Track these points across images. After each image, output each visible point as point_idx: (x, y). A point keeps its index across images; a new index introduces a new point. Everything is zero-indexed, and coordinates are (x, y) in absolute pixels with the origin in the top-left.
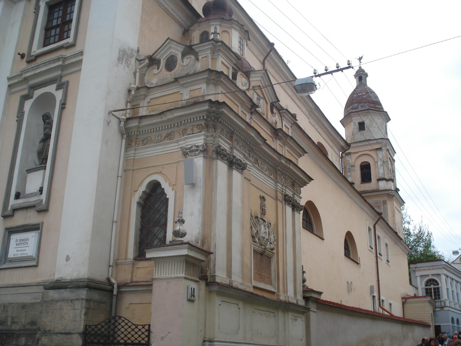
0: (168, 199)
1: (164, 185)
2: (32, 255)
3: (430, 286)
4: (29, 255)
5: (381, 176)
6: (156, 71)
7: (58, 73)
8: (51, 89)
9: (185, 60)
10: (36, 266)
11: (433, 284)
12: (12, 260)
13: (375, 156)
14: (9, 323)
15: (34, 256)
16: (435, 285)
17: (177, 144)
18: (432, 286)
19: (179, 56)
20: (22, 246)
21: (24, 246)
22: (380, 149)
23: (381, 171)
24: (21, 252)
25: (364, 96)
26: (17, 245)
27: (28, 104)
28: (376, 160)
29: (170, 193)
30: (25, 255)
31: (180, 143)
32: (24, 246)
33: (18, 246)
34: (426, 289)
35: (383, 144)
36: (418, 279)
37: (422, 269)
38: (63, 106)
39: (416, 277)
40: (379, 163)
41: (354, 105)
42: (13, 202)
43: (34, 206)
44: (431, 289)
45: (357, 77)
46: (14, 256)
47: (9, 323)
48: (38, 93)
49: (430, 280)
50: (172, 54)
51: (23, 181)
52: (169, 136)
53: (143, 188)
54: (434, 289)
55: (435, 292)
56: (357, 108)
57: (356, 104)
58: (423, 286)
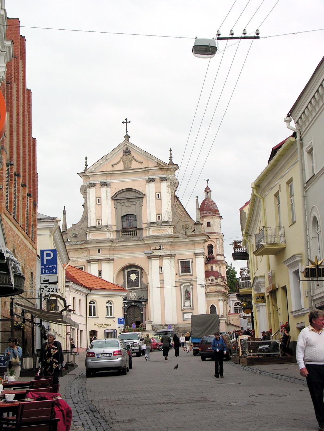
3: (237, 306)
5: (218, 253)
7: (190, 281)
8: (189, 284)
11: (239, 305)
12: (185, 319)
13: (215, 242)
14: (189, 330)
16: (239, 305)
18: (238, 306)
19: (214, 279)
22: (218, 238)
23: (218, 250)
25: (210, 207)
27: (182, 287)
28: (216, 244)
29: (216, 307)
34: (235, 308)
35: (220, 236)
36: (231, 302)
37: (233, 297)
38: (193, 289)
39: (230, 301)
40: (217, 245)
41: (205, 212)
42: (183, 307)
44: (237, 308)
45: (206, 193)
47: (189, 330)
48: (184, 285)
49: (237, 303)
51: (184, 303)
52: (215, 296)
54: (239, 307)
55: (239, 309)
56: (207, 214)
57: (206, 211)
58: (234, 306)
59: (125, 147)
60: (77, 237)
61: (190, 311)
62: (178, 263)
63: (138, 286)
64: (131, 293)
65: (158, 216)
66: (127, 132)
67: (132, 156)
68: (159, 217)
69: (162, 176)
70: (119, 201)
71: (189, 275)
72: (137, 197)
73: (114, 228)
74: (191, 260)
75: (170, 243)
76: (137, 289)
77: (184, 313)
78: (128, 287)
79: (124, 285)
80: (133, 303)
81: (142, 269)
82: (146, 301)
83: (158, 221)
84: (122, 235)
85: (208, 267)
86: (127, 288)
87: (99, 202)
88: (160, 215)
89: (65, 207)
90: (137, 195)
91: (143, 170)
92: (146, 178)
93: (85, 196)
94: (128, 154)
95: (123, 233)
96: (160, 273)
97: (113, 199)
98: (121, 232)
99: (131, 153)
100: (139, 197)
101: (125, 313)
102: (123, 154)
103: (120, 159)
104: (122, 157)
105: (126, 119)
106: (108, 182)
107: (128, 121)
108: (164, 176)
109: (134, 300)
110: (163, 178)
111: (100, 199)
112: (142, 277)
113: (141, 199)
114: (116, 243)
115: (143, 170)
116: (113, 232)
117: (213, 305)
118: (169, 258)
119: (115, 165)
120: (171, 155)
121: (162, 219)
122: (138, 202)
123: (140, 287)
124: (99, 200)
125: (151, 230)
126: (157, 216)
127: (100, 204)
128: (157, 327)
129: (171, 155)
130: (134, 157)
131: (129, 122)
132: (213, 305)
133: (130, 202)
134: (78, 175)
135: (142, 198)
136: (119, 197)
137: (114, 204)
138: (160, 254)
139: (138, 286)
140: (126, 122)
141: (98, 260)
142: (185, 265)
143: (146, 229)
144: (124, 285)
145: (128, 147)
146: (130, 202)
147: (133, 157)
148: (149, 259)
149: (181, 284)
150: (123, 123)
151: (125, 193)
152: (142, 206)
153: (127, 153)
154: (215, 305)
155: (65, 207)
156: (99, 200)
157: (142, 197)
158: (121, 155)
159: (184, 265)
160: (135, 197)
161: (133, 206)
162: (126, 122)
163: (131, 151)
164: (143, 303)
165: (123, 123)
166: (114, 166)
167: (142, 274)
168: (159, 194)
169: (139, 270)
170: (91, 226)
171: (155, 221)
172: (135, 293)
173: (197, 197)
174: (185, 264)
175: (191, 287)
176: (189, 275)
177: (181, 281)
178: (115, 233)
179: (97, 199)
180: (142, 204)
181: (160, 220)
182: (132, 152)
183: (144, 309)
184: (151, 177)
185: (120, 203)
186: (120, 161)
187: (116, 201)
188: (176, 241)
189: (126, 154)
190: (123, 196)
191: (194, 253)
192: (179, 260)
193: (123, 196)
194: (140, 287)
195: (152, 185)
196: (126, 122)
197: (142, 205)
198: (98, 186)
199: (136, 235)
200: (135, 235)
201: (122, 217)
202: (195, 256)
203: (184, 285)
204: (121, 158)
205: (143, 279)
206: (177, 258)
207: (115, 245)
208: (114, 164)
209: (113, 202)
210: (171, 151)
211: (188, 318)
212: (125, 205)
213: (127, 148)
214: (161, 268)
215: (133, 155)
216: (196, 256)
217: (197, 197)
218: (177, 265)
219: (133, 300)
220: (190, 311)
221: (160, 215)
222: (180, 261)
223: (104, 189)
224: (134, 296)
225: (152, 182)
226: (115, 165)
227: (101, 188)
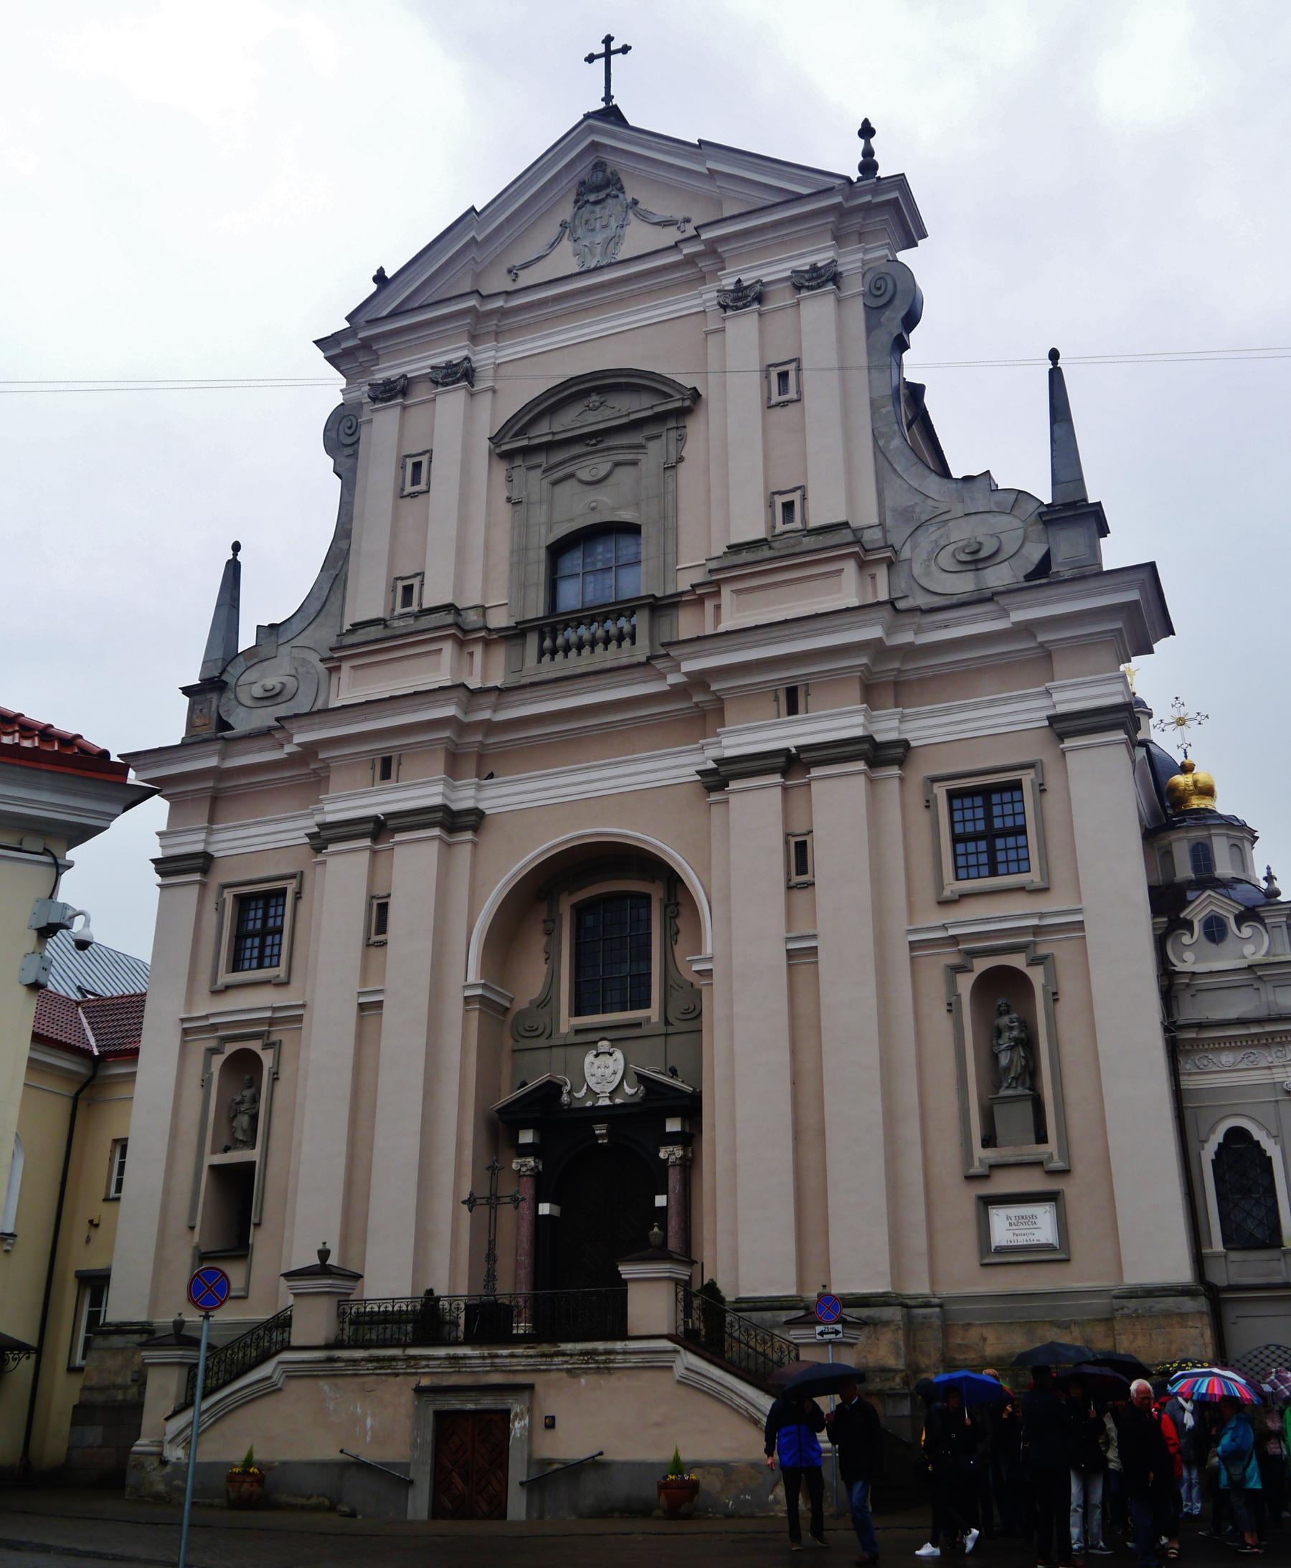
0: (1270, 1158)
1: (1258, 1134)
2: (1051, 1242)
4: (1043, 1241)
6: (1186, 939)
9: (1243, 928)
10: (1067, 1261)
12: (1001, 1250)
15: (1056, 1244)
17: (1267, 1072)
20: (1022, 1227)
21: (1027, 1227)
24: (1025, 1237)
26: (1010, 1224)
27: (965, 984)
29: (1271, 1148)
30: (1035, 1242)
31: (1274, 1071)
32: (1027, 1227)
33: (1014, 1227)
38: (1055, 997)
43: (1039, 1164)
46: (1009, 1244)
50: (1213, 913)
53: (1218, 1137)
59: (588, 162)
60: (279, 700)
61: (1033, 1182)
62: (929, 804)
63: (646, 1004)
64: (589, 1058)
65: (780, 500)
66: (608, 97)
67: (629, 200)
68: (788, 507)
69: (803, 264)
70: (541, 459)
71: (1021, 889)
72: (649, 413)
73: (499, 620)
74: (1027, 778)
75: (864, 660)
76: (639, 1025)
77: (988, 1201)
78: (578, 1011)
79: (547, 1001)
80: (600, 1130)
81: (672, 881)
82: (691, 1107)
83: (777, 531)
84: (542, 653)
85: (1167, 854)
86: (567, 1023)
87: (416, 480)
88: (796, 497)
89: (236, 547)
90: (639, 406)
91: (685, 251)
92: (705, 297)
93: (350, 462)
94: (602, 195)
95: (547, 643)
96: (789, 888)
97: (505, 448)
98: (532, 641)
99: (621, 189)
100: (657, 410)
101: (545, 1209)
102: (576, 202)
103: (559, 229)
104: (568, 219)
105: (608, 40)
106: (484, 357)
107: (614, 46)
108: (822, 259)
109: (607, 1102)
110: (814, 268)
111: (424, 459)
112: (671, 936)
113: (672, 424)
114: (492, 698)
115: (688, 250)
116: (487, 643)
117: (1237, 1136)
118: (860, 765)
119: (525, 266)
120: (868, 153)
121: (804, 520)
122: (653, 447)
123: (653, 1013)
124: (417, 466)
125: (726, 591)
126: (771, 505)
127: (422, 487)
128: (756, 1316)
129: (868, 153)
130: (641, 206)
131: (625, 49)
132: (1237, 1136)
133: (608, 449)
134: (320, 354)
135: (683, 413)
136: (542, 432)
137: (510, 480)
138: (791, 744)
139: (646, 1004)
140: (609, 51)
141: (370, 826)
142: (989, 818)
143: (700, 601)
144: (547, 1001)
145: (608, 157)
146: (608, 449)
147: (635, 202)
148: (715, 797)
149: (955, 960)
150: (591, 58)
151: (578, 408)
152: (682, 466)
153: (598, 189)
154: (1262, 1126)
155: (236, 547)
156: (417, 466)
157: (678, 404)
158: (566, 211)
159: (980, 813)
160: (633, 417)
161: (624, 474)
162: (608, 54)
163: (622, 176)
164: (673, 1126)
165: (591, 58)
166: (519, 272)
167: (677, 915)
168: (791, 368)
169: (657, 893)
170: (359, 618)
171: (757, 531)
172: (618, 1055)
173: (1054, 355)
174: (988, 807)
175: (1037, 976)
176: (1021, 889)
177: (955, 940)
178: (500, 655)
179: (410, 462)
180: (680, 450)
181: (797, 524)
182: (626, 183)
183: (674, 1178)
184: (728, 283)
185: (544, 465)
186: (558, 240)
187: (518, 462)
188: (906, 637)
189: (592, 198)
190: (570, 421)
191: (1052, 719)
192: (936, 785)
193: (570, 421)
194: (653, 1013)
195: (744, 327)
196: (609, 51)
197: (681, 459)
198: (421, 393)
199: (633, 643)
200: (626, 643)
201: (558, 550)
202: (1061, 737)
203: (982, 965)
204: (564, 225)
205: (679, 949)
206: (922, 769)
207: (486, 715)
208: (518, 263)
209: (501, 469)
210: (867, 131)
211: (1021, 1241)
212: (572, 476)
213: (599, 166)
214: (801, 848)
215: (631, 192)
216: (1068, 743)
217: (1054, 355)
218: (920, 818)
219: (604, 1102)
220: (1033, 1182)
221: (796, 497)
222: (940, 791)
223: (452, 403)
224: (608, 1072)
225: (745, 306)
226: (525, 266)
227: (434, 400)
